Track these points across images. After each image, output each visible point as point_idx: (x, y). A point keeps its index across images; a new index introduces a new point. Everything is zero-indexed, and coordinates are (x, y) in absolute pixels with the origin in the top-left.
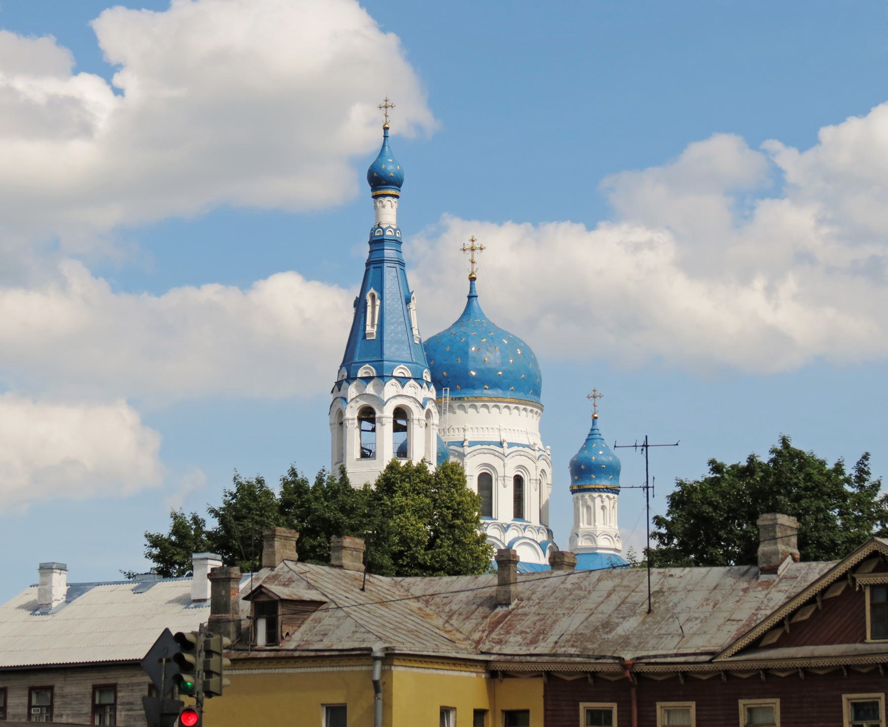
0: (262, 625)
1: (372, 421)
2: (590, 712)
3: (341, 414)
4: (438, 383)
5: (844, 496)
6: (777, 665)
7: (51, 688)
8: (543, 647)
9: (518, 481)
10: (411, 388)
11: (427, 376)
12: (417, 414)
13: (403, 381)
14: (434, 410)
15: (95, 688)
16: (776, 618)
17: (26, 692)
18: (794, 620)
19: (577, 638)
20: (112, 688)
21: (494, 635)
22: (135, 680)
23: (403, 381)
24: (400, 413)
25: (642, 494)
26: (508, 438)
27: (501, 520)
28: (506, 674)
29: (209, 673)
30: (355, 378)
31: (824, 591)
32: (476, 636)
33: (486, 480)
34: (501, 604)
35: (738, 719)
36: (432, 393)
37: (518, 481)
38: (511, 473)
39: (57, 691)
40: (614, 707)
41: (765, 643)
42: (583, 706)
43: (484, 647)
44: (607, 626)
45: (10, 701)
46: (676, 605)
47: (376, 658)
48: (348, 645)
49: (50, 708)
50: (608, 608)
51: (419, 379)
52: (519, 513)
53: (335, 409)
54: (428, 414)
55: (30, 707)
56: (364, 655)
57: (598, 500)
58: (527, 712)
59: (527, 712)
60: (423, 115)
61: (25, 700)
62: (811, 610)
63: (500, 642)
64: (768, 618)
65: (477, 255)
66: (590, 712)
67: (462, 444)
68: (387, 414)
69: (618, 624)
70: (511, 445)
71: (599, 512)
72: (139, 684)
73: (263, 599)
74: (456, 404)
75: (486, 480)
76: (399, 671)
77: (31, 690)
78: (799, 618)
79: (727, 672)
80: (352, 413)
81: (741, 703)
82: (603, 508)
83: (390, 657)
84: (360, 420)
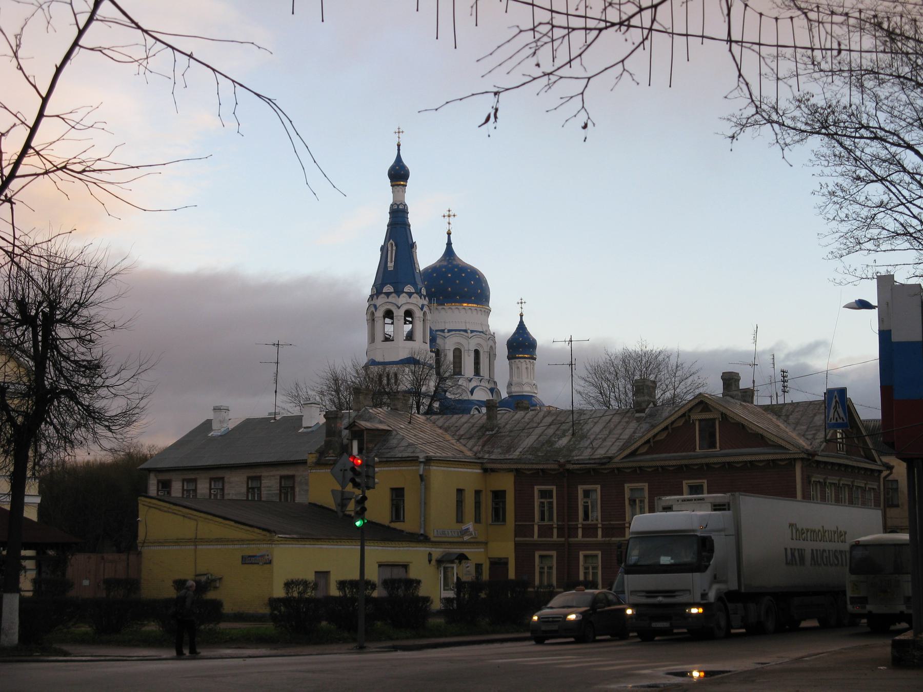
0: (355, 445)
1: (392, 318)
2: (541, 491)
3: (373, 314)
4: (430, 296)
5: (837, 443)
6: (646, 464)
7: (223, 478)
8: (516, 454)
9: (477, 352)
10: (415, 299)
11: (424, 292)
12: (418, 314)
13: (410, 295)
14: (428, 312)
15: (249, 478)
16: (646, 438)
17: (208, 481)
18: (656, 439)
19: (533, 450)
20: (259, 478)
21: (486, 449)
22: (272, 473)
23: (410, 295)
24: (408, 313)
25: (569, 368)
26: (470, 327)
27: (466, 376)
28: (493, 470)
29: (368, 476)
30: (382, 293)
31: (673, 423)
32: (475, 449)
33: (458, 353)
34: (488, 430)
35: (624, 494)
36: (426, 302)
37: (477, 352)
38: (473, 348)
39: (226, 479)
40: (554, 488)
41: (639, 452)
42: (536, 488)
43: (480, 455)
44: (550, 442)
45: (199, 486)
46: (588, 431)
47: (421, 462)
48: (405, 455)
49: (223, 489)
50: (551, 431)
51: (419, 292)
52: (477, 372)
53: (370, 312)
54: (425, 314)
55: (210, 489)
56: (414, 460)
57: (524, 366)
58: (505, 491)
59: (505, 491)
60: (878, 415)
61: (208, 486)
62: (664, 435)
63: (489, 452)
64: (641, 437)
65: (452, 219)
66: (541, 491)
67: (443, 331)
68: (399, 313)
69: (556, 442)
70: (472, 331)
71: (524, 370)
72: (274, 476)
73: (356, 429)
74: (440, 307)
75: (458, 353)
76: (434, 469)
77: (211, 479)
78: (658, 438)
79: (618, 469)
80: (379, 314)
81: (626, 485)
82: (527, 368)
83: (429, 461)
84: (384, 317)
